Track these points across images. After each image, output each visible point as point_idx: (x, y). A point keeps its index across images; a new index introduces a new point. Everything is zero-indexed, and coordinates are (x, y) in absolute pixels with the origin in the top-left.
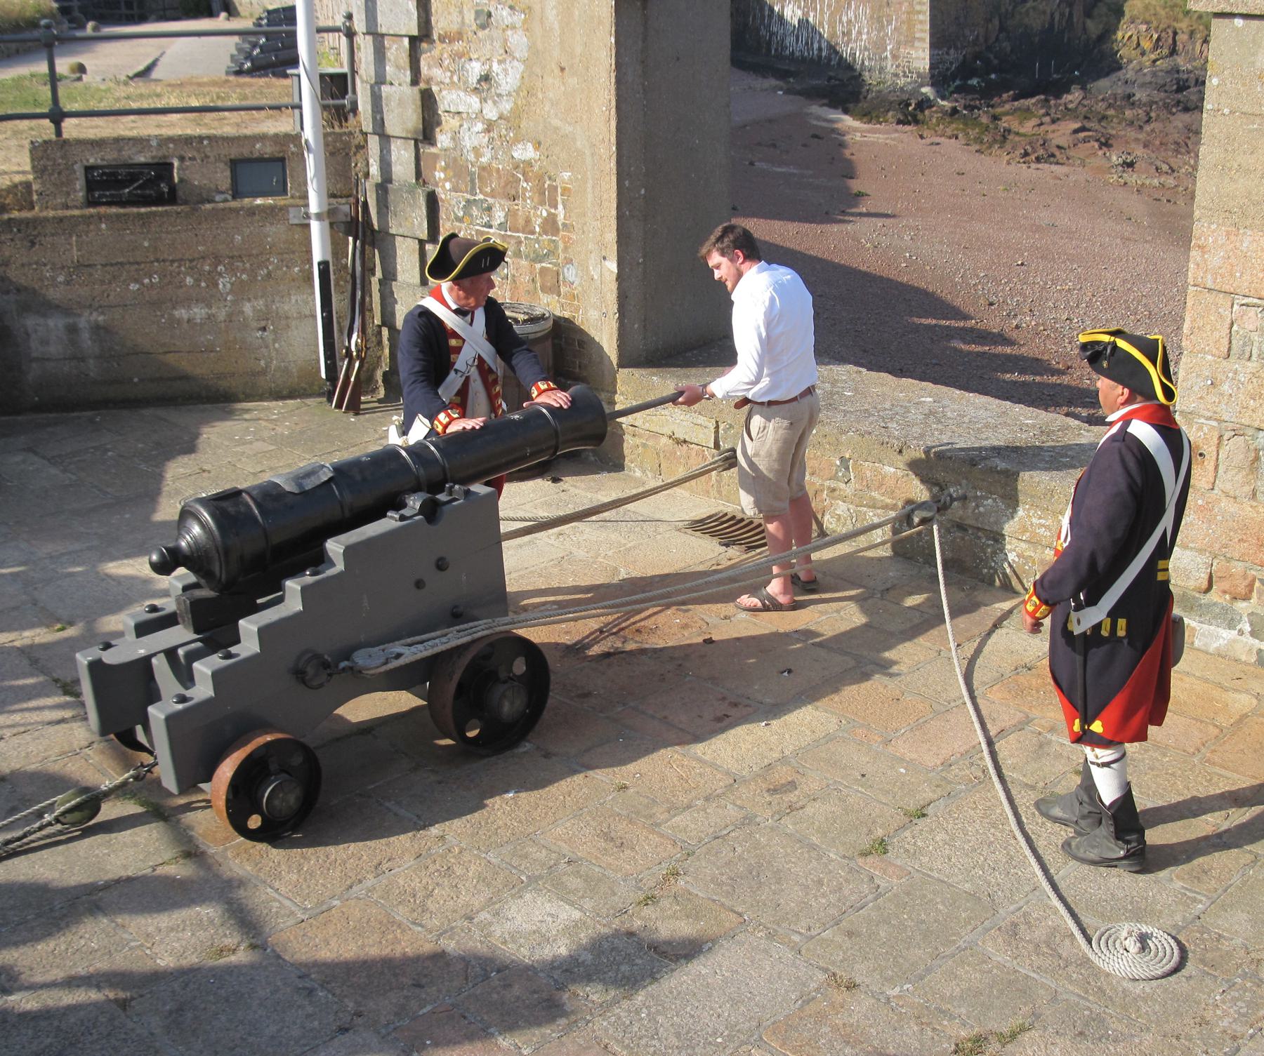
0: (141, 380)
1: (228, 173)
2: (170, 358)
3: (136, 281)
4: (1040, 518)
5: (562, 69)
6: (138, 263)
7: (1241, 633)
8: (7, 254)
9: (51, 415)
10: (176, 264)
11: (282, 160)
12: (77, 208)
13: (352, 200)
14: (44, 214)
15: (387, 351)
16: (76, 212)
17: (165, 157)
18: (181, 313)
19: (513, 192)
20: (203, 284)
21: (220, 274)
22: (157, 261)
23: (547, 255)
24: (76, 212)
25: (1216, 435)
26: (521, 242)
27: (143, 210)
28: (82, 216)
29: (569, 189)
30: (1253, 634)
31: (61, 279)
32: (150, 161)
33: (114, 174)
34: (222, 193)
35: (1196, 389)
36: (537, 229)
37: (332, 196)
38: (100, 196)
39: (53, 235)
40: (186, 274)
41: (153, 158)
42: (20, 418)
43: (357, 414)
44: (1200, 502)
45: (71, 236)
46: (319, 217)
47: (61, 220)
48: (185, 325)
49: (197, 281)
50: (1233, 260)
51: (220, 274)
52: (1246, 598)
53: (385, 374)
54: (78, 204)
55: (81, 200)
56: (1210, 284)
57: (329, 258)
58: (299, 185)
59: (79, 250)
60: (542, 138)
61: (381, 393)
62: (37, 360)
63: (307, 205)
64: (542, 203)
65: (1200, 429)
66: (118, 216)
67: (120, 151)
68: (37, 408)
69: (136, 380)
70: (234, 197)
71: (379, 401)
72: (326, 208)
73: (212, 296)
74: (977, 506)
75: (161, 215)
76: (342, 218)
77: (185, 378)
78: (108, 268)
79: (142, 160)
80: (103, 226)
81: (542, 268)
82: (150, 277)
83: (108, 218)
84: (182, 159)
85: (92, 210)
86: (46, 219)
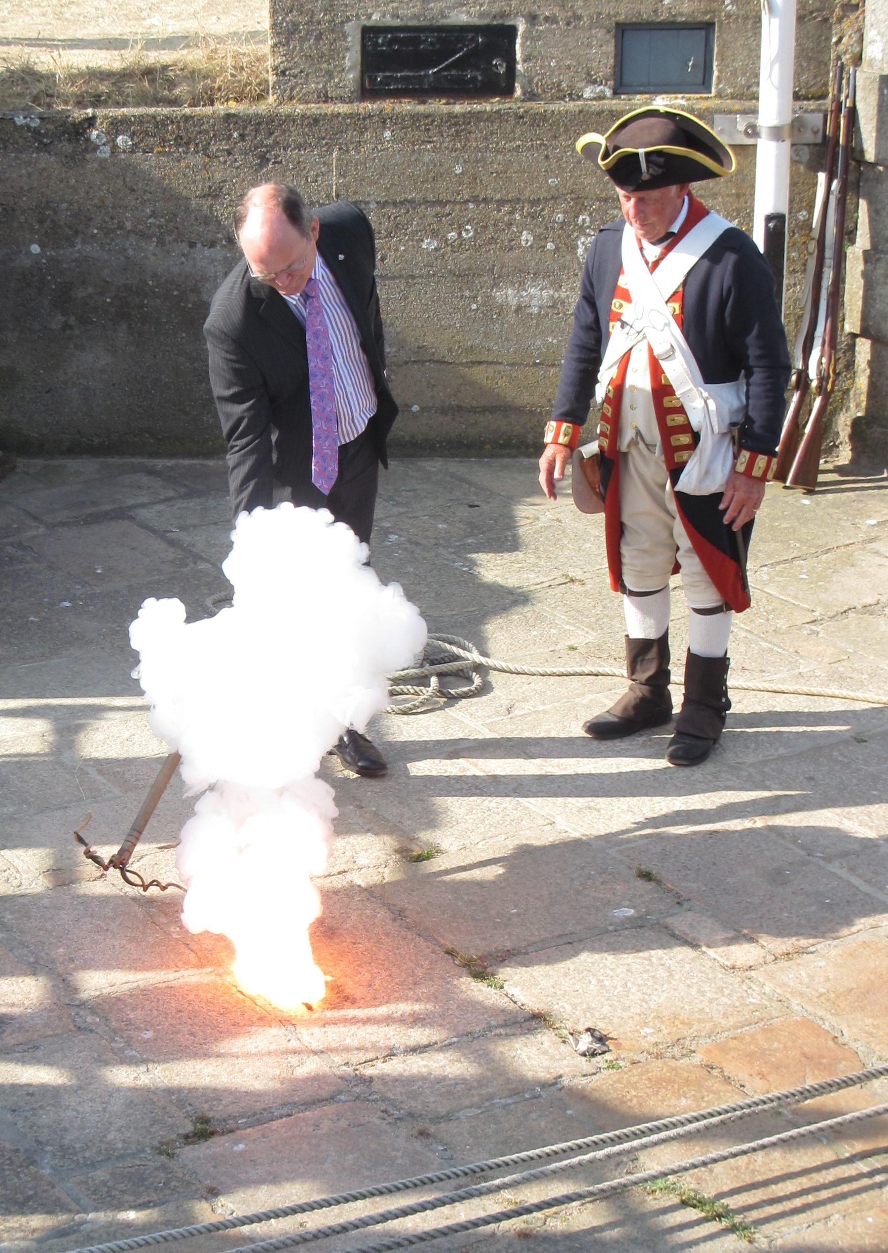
0: (423, 409)
1: (610, 48)
2: (480, 374)
3: (435, 234)
6: (440, 203)
8: (218, 176)
11: (708, 26)
12: (342, 99)
13: (828, 103)
14: (286, 109)
15: (862, 382)
16: (343, 108)
17: (503, 15)
20: (550, 246)
21: (581, 229)
22: (475, 200)
24: (343, 108)
28: (351, 116)
32: (477, 21)
33: (416, 41)
34: (594, 82)
37: (797, 97)
38: (387, 81)
39: (299, 147)
40: (523, 226)
41: (481, 15)
42: (211, 463)
43: (810, 492)
46: (776, 133)
47: (316, 120)
48: (511, 318)
49: (540, 239)
51: (581, 229)
53: (856, 423)
54: (346, 92)
57: (784, 209)
58: (734, 73)
59: (341, 175)
61: (845, 455)
63: (754, 112)
66: (415, 117)
69: (415, 408)
70: (616, 93)
71: (839, 470)
72: (787, 119)
73: (563, 268)
76: (809, 137)
77: (503, 408)
78: (390, 210)
80: (387, 134)
82: (460, 228)
83: (396, 119)
84: (532, 19)
85: (369, 106)
86: (290, 119)
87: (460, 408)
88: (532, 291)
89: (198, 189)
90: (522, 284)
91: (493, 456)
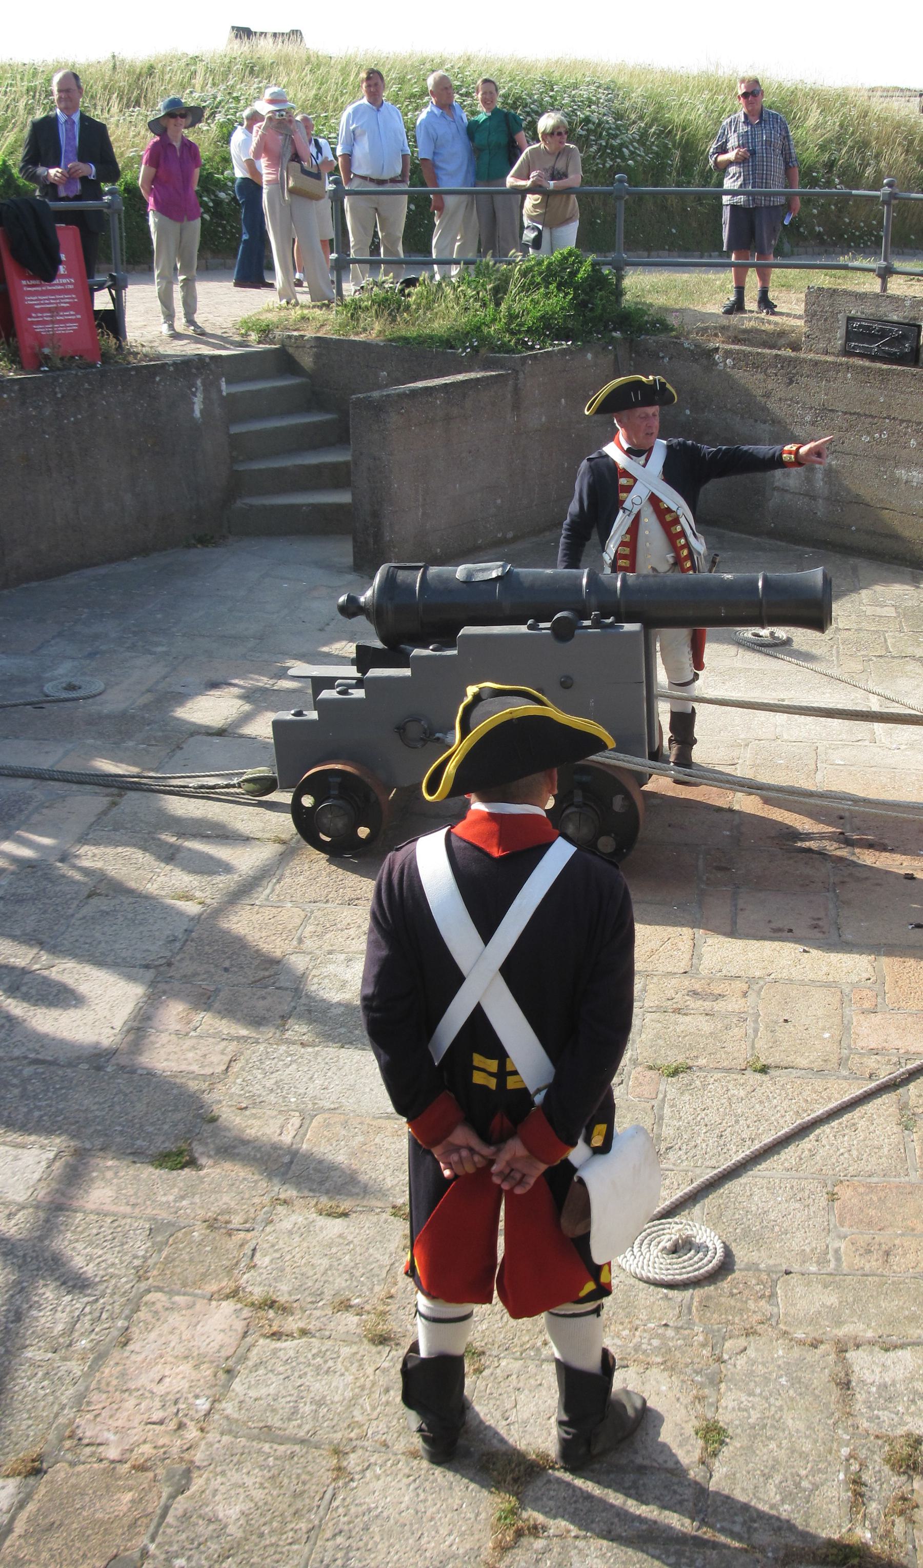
3: (868, 433)
8: (770, 387)
9: (779, 543)
10: (904, 425)
12: (833, 354)
17: (915, 319)
18: (901, 473)
22: (888, 417)
24: (830, 359)
27: (885, 367)
28: (832, 363)
31: (808, 418)
32: (901, 320)
41: (904, 318)
45: (822, 380)
47: (816, 363)
55: (839, 348)
62: (777, 489)
66: (863, 368)
67: (878, 306)
68: (773, 534)
75: (899, 374)
77: (896, 537)
79: (895, 318)
85: (844, 359)
86: (805, 361)
87: (875, 532)
88: (914, 473)
89: (760, 392)
90: (909, 468)
91: (889, 563)
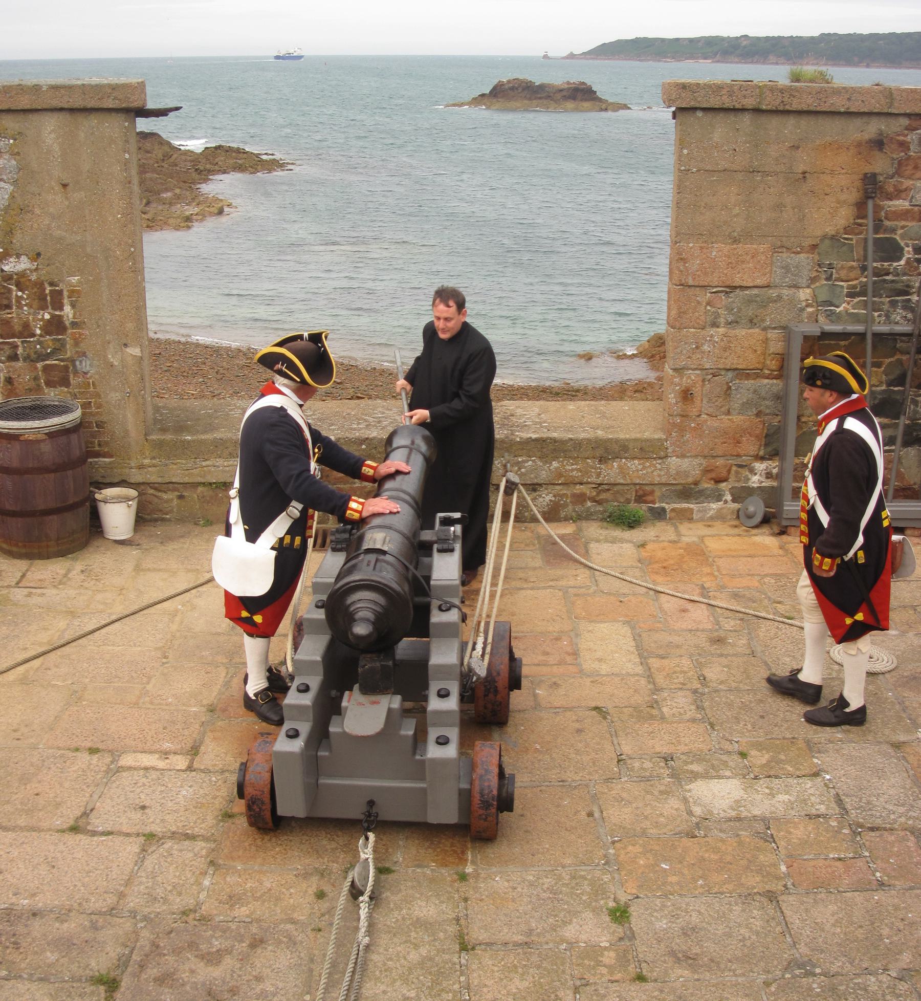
4: (573, 465)
5: (65, 186)
7: (726, 502)
19: (5, 302)
23: (52, 353)
25: (701, 378)
26: (17, 347)
29: (78, 292)
30: (734, 501)
35: (684, 352)
36: (38, 332)
44: (693, 425)
50: (706, 265)
52: (725, 480)
56: (691, 282)
60: (41, 249)
64: (44, 308)
65: (689, 377)
74: (520, 469)
81: (46, 368)
